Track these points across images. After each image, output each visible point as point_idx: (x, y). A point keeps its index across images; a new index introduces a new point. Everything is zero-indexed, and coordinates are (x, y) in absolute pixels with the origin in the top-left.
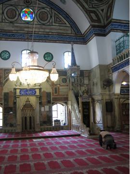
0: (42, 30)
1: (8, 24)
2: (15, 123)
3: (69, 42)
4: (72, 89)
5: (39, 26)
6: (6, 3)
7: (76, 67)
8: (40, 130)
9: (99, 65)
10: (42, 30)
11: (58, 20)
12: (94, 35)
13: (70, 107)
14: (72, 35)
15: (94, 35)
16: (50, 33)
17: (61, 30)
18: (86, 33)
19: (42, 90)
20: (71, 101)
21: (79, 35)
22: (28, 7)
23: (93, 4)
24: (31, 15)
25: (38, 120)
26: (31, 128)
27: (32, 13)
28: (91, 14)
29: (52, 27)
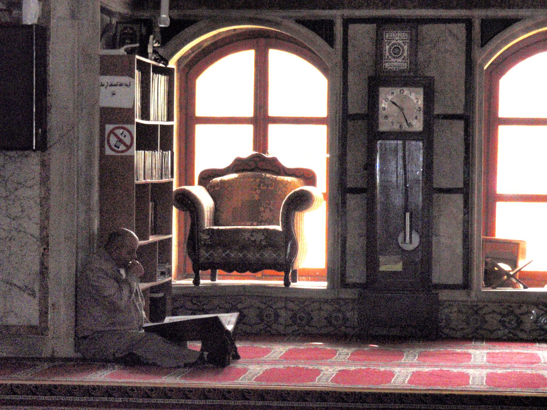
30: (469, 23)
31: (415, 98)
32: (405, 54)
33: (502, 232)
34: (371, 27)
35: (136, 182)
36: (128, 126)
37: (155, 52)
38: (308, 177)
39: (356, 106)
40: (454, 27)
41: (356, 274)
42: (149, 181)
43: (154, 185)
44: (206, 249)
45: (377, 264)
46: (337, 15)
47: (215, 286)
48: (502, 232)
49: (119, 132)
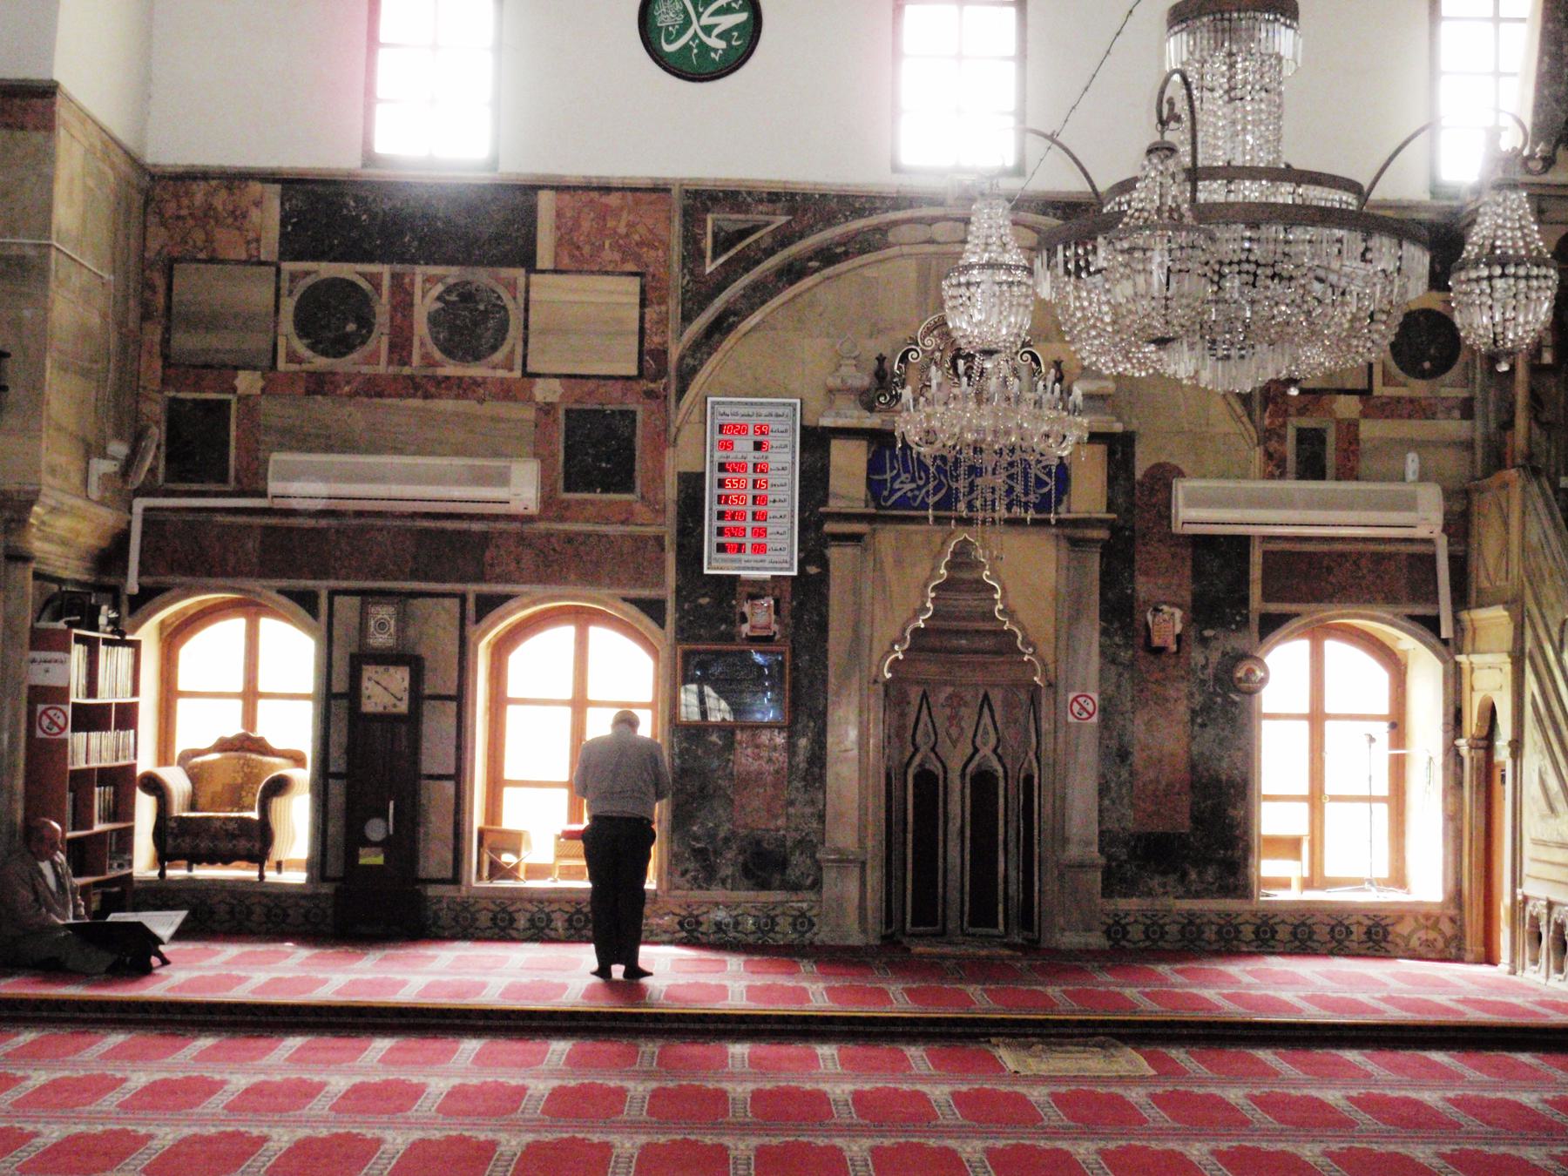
2: (807, 845)
4: (1530, 456)
8: (1097, 940)
13: (1490, 678)
19: (1143, 463)
20: (1515, 604)
25: (1079, 809)
26: (982, 911)
30: (463, 598)
31: (399, 678)
32: (392, 630)
33: (508, 822)
34: (356, 600)
35: (70, 767)
36: (63, 707)
37: (111, 622)
38: (297, 759)
39: (340, 685)
40: (447, 602)
41: (335, 868)
42: (94, 764)
43: (102, 771)
44: (176, 839)
45: (357, 856)
46: (322, 586)
47: (192, 880)
48: (508, 822)
49: (51, 713)
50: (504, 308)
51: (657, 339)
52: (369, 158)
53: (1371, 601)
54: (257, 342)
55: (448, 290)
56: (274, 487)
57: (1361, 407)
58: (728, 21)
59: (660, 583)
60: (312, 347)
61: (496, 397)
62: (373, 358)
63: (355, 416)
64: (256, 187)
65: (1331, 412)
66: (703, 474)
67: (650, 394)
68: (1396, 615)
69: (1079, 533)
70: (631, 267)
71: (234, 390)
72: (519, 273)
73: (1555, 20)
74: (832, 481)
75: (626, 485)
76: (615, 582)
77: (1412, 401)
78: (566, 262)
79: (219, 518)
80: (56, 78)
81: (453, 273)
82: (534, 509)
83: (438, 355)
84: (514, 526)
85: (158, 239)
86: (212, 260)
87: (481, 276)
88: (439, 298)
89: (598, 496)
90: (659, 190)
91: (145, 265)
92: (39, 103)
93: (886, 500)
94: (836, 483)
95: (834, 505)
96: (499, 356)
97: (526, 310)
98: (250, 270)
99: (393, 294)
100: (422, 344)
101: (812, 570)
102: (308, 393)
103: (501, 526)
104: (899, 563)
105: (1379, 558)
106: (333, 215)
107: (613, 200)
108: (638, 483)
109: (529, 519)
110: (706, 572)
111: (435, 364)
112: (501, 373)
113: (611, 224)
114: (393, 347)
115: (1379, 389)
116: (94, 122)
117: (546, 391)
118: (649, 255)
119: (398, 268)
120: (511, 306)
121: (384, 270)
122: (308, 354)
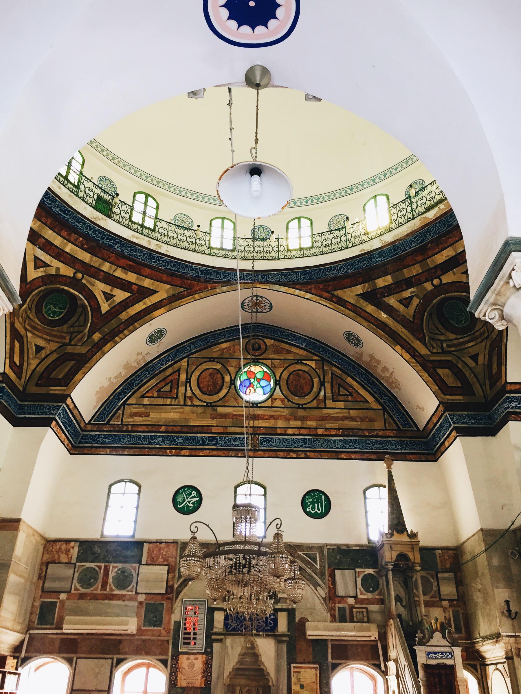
0: (298, 424)
1: (200, 410)
3: (379, 457)
5: (286, 412)
6: (194, 356)
7: (404, 538)
9: (482, 530)
10: (298, 424)
11: (343, 391)
12: (454, 433)
14: (388, 433)
15: (454, 433)
16: (320, 432)
17: (353, 419)
18: (431, 426)
20: (395, 661)
21: (409, 434)
22: (256, 362)
23: (442, 342)
24: (264, 383)
27: (266, 377)
28: (440, 371)
29: (325, 411)
30: (112, 659)
50: (132, 575)
51: (171, 583)
52: (102, 536)
53: (361, 660)
54: (65, 585)
55: (119, 570)
56: (65, 626)
57: (354, 601)
58: (194, 500)
59: (167, 654)
60: (81, 586)
61: (128, 600)
62: (96, 589)
63: (91, 605)
64: (72, 544)
65: (347, 603)
66: (180, 622)
67: (168, 599)
68: (369, 664)
69: (280, 638)
70: (166, 563)
71: (59, 598)
72: (137, 565)
73: (391, 499)
74: (214, 623)
75: (160, 625)
76: (154, 654)
77: (368, 599)
78: (149, 562)
79: (50, 636)
80: (22, 517)
81: (120, 565)
82: (135, 632)
83: (114, 588)
84: (129, 638)
85: (46, 557)
86: (59, 563)
87: (127, 566)
88: (116, 572)
89: (152, 628)
90: (175, 542)
91: (42, 564)
92: (15, 524)
93: (229, 628)
94: (216, 624)
95: (215, 630)
96: (129, 588)
97: (138, 575)
98: (69, 565)
99: (104, 571)
100: (110, 585)
101: (209, 650)
102: (79, 599)
103: (125, 638)
104: (232, 647)
105: (363, 646)
106: (93, 550)
107: (163, 545)
108: (163, 623)
109: (132, 635)
110: (180, 651)
111: (113, 591)
112: (130, 593)
113: (162, 551)
114: (102, 586)
115: (359, 596)
116: (31, 528)
117: (141, 598)
118: (170, 560)
119: (106, 564)
120: (134, 573)
121: (103, 565)
122: (80, 588)
